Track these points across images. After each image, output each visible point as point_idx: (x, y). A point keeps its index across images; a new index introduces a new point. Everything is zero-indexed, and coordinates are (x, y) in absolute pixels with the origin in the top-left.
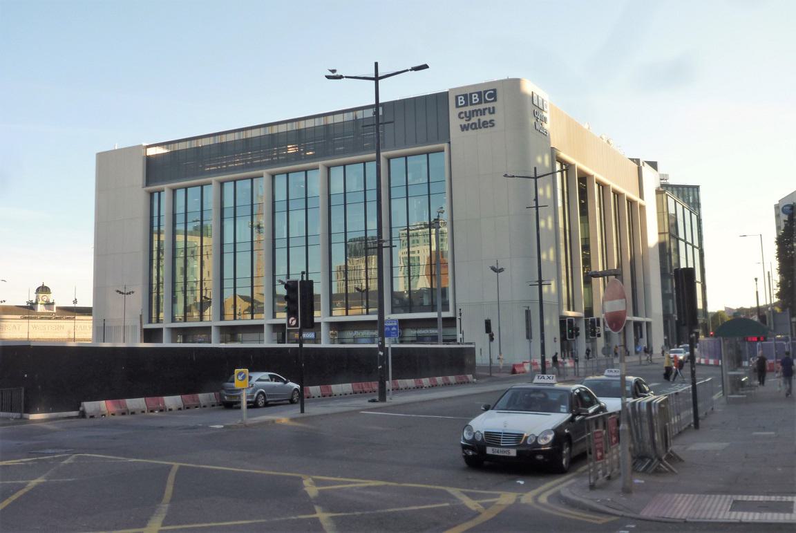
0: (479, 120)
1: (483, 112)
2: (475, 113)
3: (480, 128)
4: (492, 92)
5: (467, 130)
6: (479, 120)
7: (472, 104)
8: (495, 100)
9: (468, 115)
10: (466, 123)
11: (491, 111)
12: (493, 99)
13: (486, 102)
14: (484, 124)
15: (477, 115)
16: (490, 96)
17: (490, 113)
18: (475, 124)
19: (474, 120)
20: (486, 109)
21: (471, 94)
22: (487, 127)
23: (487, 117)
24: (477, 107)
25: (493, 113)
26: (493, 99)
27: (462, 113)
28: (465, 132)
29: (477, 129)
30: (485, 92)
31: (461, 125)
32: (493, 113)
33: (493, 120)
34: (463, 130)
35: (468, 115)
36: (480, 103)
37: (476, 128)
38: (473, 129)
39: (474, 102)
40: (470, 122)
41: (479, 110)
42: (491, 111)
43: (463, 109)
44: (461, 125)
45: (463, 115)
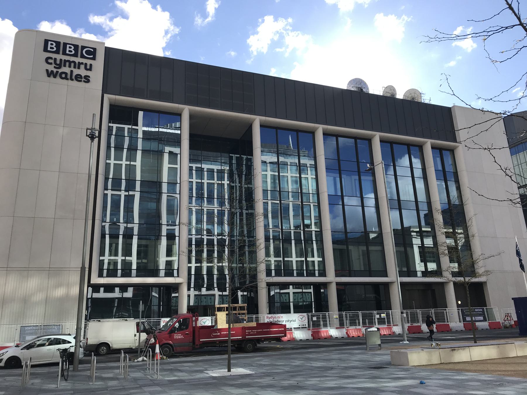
0: (72, 71)
1: (78, 66)
2: (67, 64)
3: (72, 80)
4: (92, 50)
5: (55, 77)
6: (72, 71)
7: (64, 53)
8: (94, 59)
9: (58, 62)
10: (55, 70)
11: (88, 67)
12: (92, 56)
13: (83, 56)
14: (78, 78)
15: (70, 67)
16: (88, 52)
17: (86, 69)
18: (66, 74)
19: (66, 69)
20: (82, 63)
21: (65, 44)
22: (81, 81)
23: (82, 72)
24: (72, 59)
25: (90, 69)
26: (92, 56)
27: (51, 58)
28: (52, 78)
29: (67, 79)
30: (83, 47)
31: (47, 70)
32: (90, 69)
33: (89, 77)
34: (49, 75)
35: (58, 62)
36: (75, 55)
37: (66, 78)
38: (62, 78)
39: (67, 52)
40: (60, 71)
41: (74, 62)
42: (88, 67)
43: (54, 56)
44: (47, 70)
45: (50, 61)
